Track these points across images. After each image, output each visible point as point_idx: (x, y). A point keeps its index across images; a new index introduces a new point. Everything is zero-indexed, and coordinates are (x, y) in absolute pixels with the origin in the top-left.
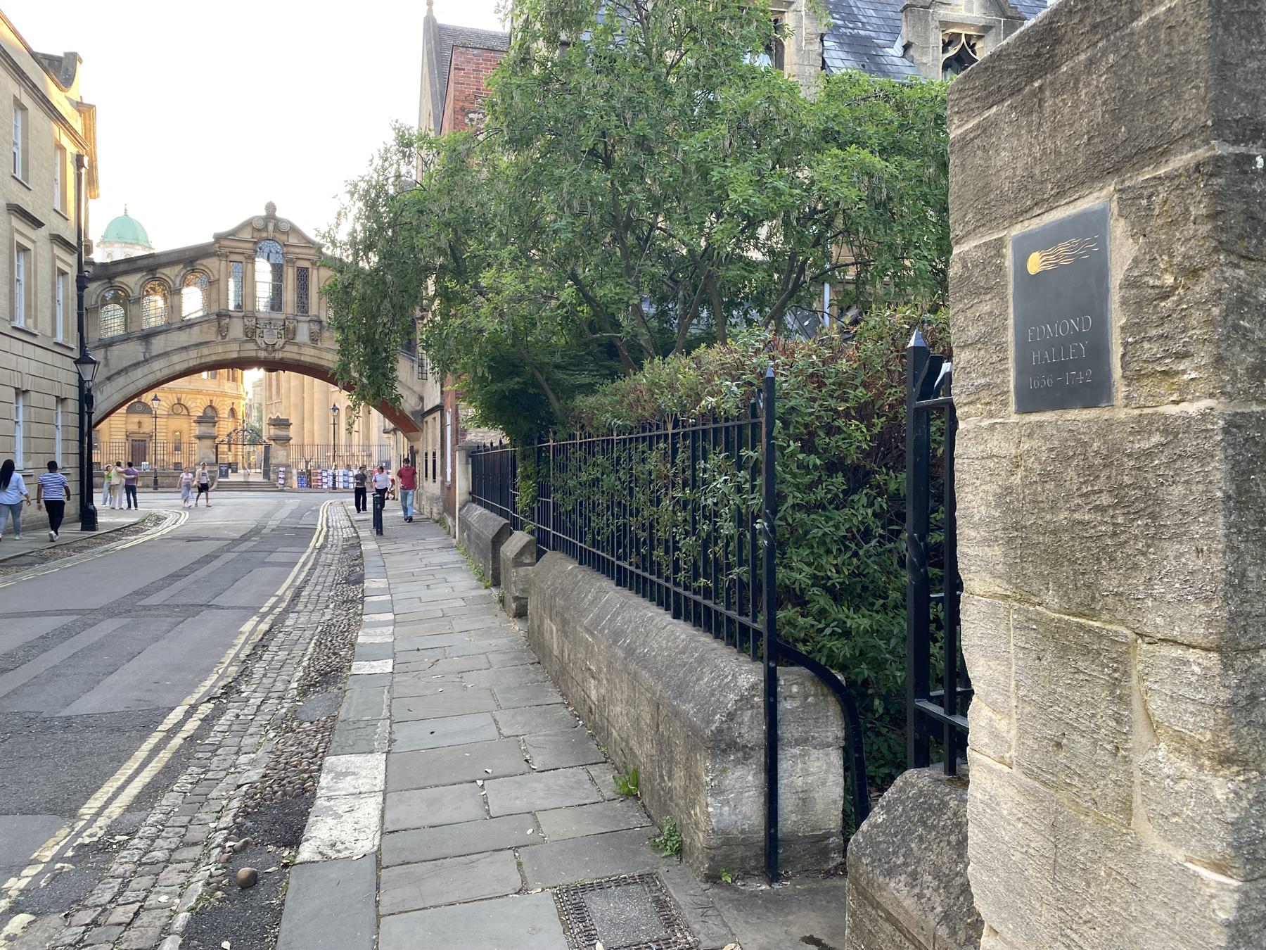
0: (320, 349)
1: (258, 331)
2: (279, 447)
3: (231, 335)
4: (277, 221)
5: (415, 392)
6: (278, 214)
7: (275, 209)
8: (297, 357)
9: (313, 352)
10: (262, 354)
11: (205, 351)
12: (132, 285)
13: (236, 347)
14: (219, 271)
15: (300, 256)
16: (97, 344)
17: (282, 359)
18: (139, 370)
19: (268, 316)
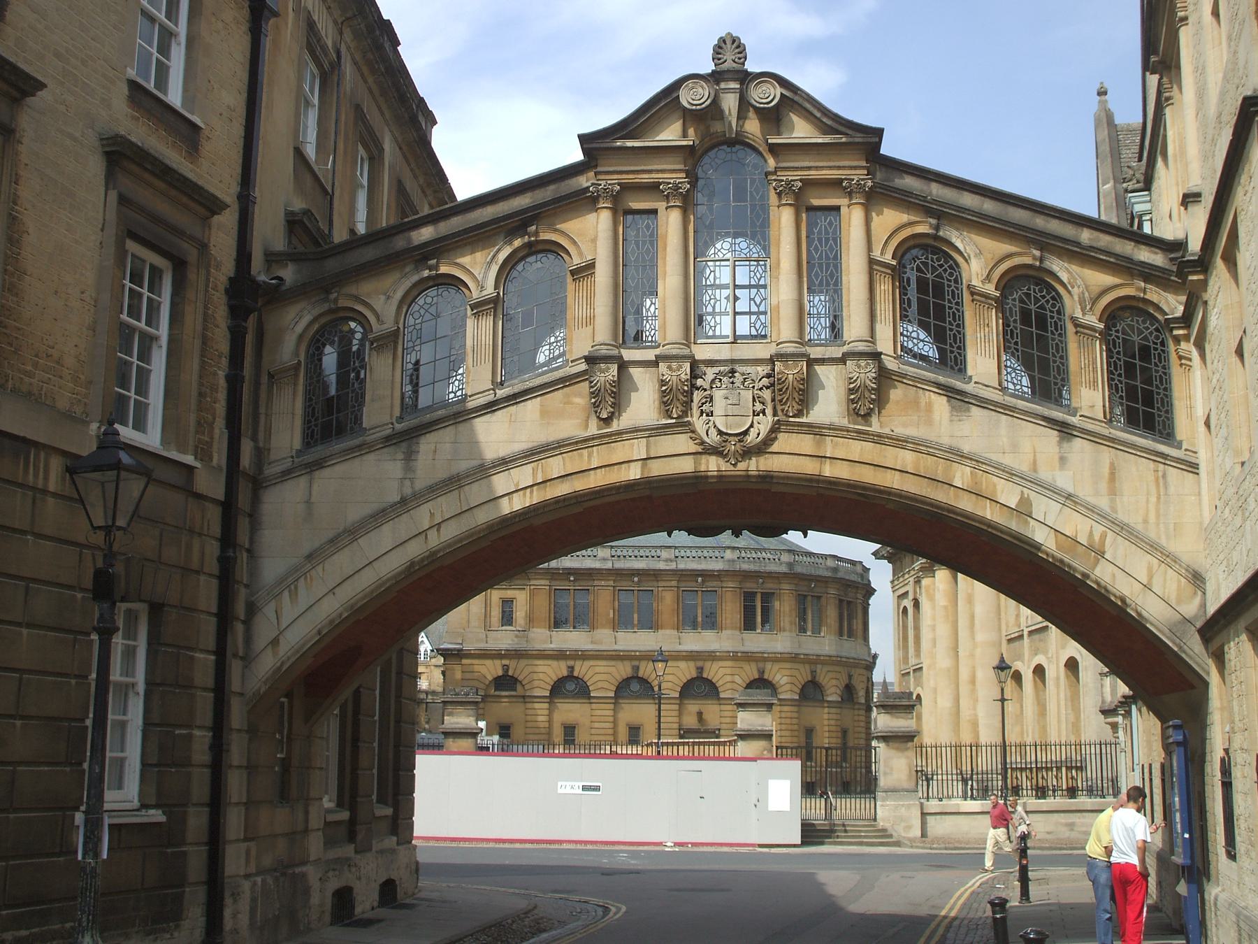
0: (878, 439)
1: (697, 396)
2: (892, 753)
3: (625, 420)
4: (745, 78)
5: (1176, 560)
6: (752, 66)
7: (740, 48)
8: (809, 467)
9: (857, 449)
10: (713, 465)
11: (556, 466)
12: (378, 303)
13: (638, 449)
14: (594, 240)
15: (814, 174)
16: (287, 464)
17: (767, 478)
18: (387, 529)
19: (724, 353)
